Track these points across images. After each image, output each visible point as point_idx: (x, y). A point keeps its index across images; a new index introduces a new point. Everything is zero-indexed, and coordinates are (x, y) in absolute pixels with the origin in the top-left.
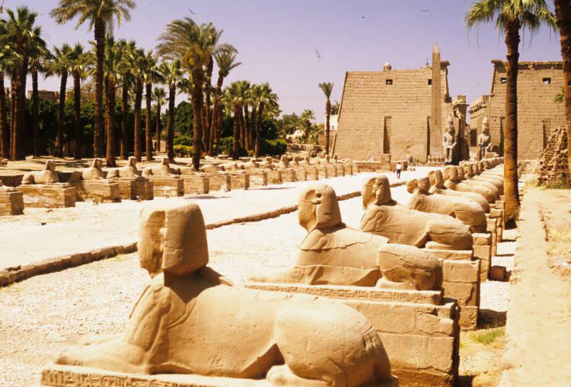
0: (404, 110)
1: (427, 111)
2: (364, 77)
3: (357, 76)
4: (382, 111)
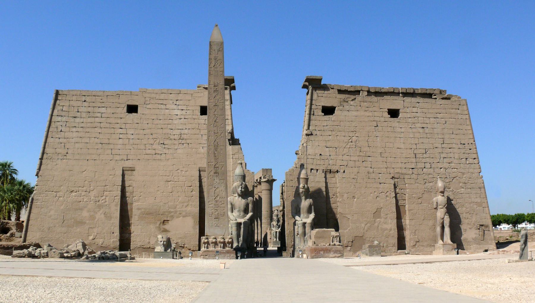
0: (158, 157)
1: (200, 157)
2: (88, 99)
3: (74, 98)
4: (118, 158)
